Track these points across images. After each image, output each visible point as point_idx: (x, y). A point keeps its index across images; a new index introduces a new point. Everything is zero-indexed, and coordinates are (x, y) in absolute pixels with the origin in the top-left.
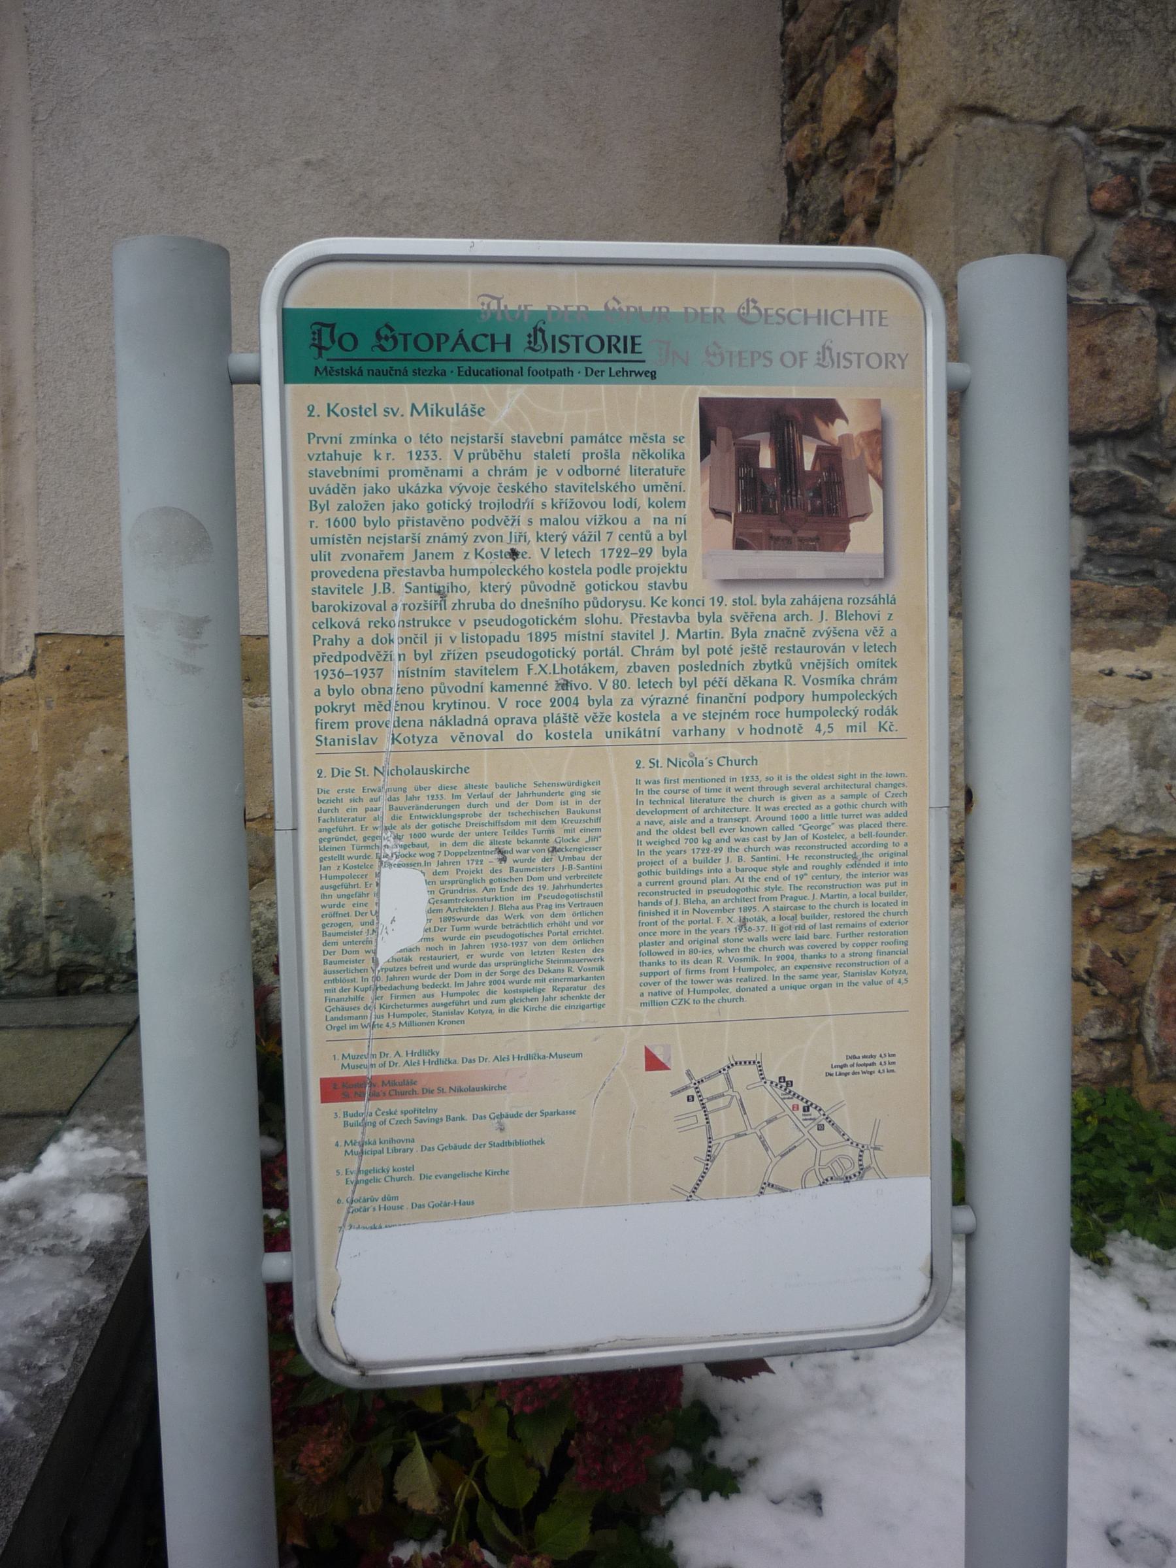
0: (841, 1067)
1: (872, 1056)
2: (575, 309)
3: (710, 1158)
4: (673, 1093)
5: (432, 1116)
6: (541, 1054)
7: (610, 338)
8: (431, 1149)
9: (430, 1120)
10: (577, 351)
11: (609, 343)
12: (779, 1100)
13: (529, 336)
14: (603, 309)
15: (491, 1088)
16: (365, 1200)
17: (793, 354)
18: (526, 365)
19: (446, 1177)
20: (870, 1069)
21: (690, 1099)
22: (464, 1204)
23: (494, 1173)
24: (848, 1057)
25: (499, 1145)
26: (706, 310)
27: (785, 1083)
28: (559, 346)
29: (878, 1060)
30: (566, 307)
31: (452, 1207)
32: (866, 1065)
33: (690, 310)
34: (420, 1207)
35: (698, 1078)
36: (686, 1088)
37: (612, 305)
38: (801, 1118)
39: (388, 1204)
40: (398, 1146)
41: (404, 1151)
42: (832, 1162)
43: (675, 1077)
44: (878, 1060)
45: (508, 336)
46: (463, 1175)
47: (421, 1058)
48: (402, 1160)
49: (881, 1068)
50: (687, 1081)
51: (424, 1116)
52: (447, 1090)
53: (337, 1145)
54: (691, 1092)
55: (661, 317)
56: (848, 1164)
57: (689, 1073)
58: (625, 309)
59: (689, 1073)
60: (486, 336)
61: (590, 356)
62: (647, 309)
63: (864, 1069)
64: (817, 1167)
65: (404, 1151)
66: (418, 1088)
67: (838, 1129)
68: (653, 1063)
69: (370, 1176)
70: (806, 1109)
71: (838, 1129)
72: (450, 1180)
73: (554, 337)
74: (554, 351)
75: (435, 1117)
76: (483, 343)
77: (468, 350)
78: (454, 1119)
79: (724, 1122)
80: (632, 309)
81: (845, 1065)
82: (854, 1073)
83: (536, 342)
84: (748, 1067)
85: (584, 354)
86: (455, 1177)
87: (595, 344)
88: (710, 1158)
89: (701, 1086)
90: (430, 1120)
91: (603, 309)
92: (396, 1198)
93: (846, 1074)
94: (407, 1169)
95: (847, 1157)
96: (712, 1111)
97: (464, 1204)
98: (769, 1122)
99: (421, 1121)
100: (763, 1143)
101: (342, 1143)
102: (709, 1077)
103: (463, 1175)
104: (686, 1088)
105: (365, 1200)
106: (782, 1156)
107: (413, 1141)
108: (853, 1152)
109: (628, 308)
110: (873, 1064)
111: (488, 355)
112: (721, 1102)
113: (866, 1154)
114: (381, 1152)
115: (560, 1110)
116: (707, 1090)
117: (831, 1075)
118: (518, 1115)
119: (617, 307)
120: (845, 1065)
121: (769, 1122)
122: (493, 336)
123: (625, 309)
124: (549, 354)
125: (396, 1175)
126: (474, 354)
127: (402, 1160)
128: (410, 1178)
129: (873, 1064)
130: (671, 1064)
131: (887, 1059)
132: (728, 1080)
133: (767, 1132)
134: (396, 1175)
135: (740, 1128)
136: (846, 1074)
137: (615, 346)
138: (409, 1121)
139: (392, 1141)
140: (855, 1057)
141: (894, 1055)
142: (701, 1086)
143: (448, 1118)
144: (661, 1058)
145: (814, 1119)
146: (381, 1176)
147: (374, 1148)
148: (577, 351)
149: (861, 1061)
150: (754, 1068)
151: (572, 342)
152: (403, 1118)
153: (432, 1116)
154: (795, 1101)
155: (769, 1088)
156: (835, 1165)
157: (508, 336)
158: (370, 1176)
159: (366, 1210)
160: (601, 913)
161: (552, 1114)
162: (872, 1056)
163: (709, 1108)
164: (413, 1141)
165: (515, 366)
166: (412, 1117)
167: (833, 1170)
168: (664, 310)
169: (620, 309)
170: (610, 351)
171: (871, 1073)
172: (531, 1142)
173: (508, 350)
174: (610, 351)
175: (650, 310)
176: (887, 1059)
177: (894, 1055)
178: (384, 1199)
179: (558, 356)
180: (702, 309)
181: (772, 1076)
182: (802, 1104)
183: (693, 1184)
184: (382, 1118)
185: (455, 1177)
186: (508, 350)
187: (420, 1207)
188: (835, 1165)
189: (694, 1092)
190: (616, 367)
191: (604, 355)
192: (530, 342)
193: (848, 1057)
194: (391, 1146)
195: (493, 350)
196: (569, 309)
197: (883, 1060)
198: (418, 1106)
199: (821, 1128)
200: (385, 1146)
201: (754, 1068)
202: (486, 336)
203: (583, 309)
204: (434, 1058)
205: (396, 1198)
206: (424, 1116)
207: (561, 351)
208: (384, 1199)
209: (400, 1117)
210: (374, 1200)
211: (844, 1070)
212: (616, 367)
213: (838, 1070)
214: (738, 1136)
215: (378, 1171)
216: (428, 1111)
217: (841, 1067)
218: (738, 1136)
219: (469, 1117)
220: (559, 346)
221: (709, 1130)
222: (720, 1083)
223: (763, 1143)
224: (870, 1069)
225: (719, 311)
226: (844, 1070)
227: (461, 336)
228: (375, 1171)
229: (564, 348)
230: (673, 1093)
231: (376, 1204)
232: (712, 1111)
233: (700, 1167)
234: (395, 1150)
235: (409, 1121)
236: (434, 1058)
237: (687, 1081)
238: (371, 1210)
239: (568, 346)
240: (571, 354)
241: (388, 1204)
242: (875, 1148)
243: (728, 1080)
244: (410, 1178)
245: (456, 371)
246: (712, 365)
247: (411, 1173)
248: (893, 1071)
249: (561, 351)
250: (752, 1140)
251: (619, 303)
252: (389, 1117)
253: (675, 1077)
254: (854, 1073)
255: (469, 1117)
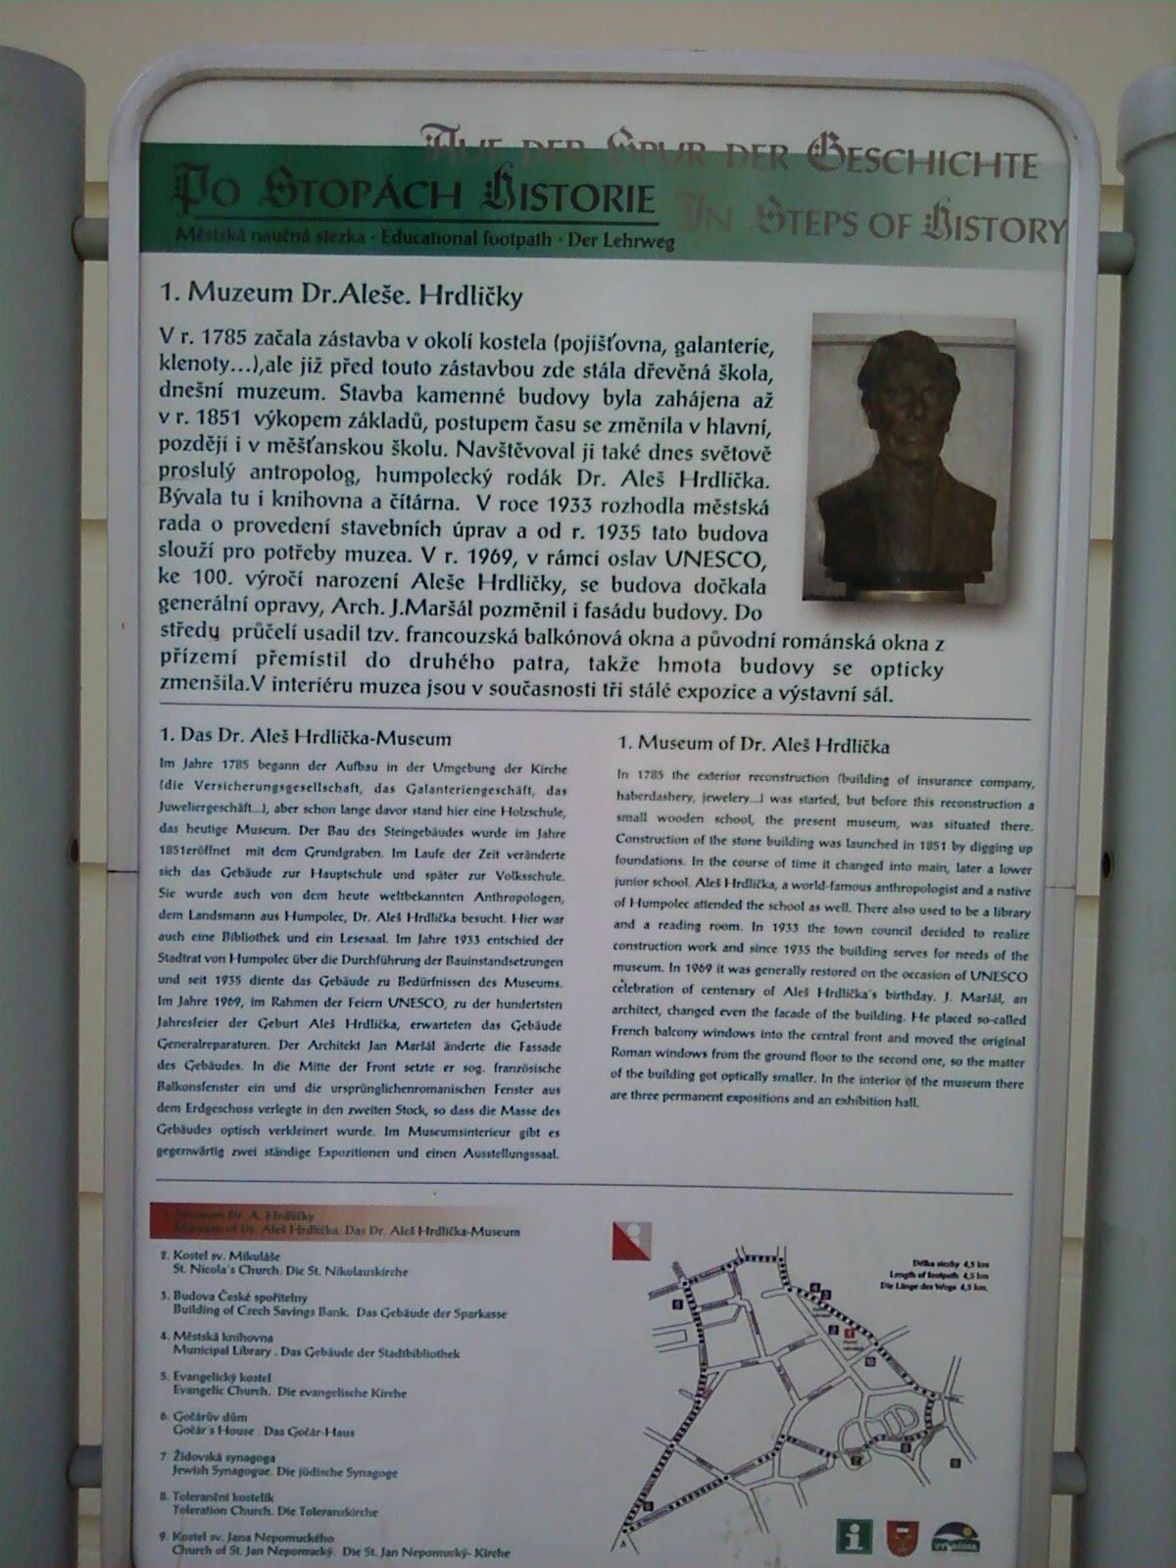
0: (905, 1276)
1: (952, 1264)
2: (564, 145)
3: (704, 1392)
4: (652, 1295)
5: (298, 1306)
6: (460, 1228)
7: (607, 188)
8: (296, 1353)
9: (295, 1312)
10: (559, 208)
11: (606, 196)
12: (808, 1316)
13: (489, 185)
14: (605, 146)
15: (386, 1273)
16: (200, 1418)
17: (890, 217)
18: (481, 229)
19: (316, 1393)
20: (949, 1282)
21: (677, 1305)
22: (341, 1434)
23: (384, 1394)
24: (916, 1263)
25: (392, 1355)
26: (760, 150)
27: (820, 1293)
28: (531, 200)
29: (961, 1270)
30: (551, 143)
31: (322, 1437)
32: (942, 1276)
33: (736, 149)
34: (277, 1433)
35: (690, 1274)
36: (672, 1288)
37: (620, 140)
38: (842, 1346)
39: (233, 1425)
40: (249, 1345)
41: (259, 1352)
42: (889, 1411)
43: (654, 1272)
44: (961, 1270)
45: (458, 186)
46: (340, 1393)
47: (288, 1224)
48: (250, 1365)
49: (966, 1283)
50: (673, 1279)
51: (289, 1306)
52: (321, 1270)
53: (164, 1336)
54: (680, 1294)
55: (692, 157)
56: (908, 1418)
57: (676, 1267)
58: (638, 147)
59: (676, 1267)
60: (424, 184)
61: (578, 216)
62: (672, 145)
63: (940, 1281)
64: (862, 1420)
65: (259, 1352)
66: (281, 1266)
67: (897, 1367)
68: (625, 1248)
69: (208, 1385)
70: (850, 1334)
71: (897, 1367)
72: (322, 1399)
73: (524, 187)
74: (524, 207)
75: (304, 1308)
76: (421, 195)
77: (397, 204)
78: (331, 1314)
79: (728, 1341)
80: (649, 147)
81: (912, 1275)
82: (925, 1287)
83: (498, 195)
84: (764, 1264)
85: (569, 212)
86: (328, 1395)
87: (585, 198)
88: (704, 1392)
89: (694, 1288)
90: (295, 1312)
91: (605, 146)
92: (244, 1418)
93: (913, 1288)
94: (260, 1378)
95: (915, 1414)
96: (710, 1326)
97: (341, 1434)
98: (793, 1347)
99: (284, 1312)
100: (784, 1377)
101: (170, 1335)
102: (708, 1275)
103: (340, 1393)
104: (672, 1288)
105: (200, 1418)
106: (812, 1398)
107: (271, 1339)
108: (920, 1403)
109: (643, 144)
110: (954, 1275)
111: (427, 211)
112: (728, 1312)
113: (937, 1407)
114: (225, 1351)
115: (485, 1311)
116: (704, 1293)
117: (890, 1287)
118: (423, 1314)
119: (626, 143)
120: (912, 1275)
121: (793, 1347)
122: (435, 185)
123: (638, 147)
124: (516, 213)
125: (244, 1385)
126: (405, 211)
127: (250, 1365)
128: (264, 1392)
129: (954, 1275)
130: (655, 1252)
131: (976, 1270)
132: (735, 1282)
133: (791, 1362)
134: (244, 1385)
135: (750, 1353)
136: (913, 1288)
137: (615, 201)
138: (266, 1311)
139: (241, 1337)
140: (926, 1263)
141: (987, 1265)
142: (694, 1288)
143: (322, 1310)
144: (637, 1242)
145: (862, 1350)
146: (224, 1385)
147: (214, 1345)
148: (559, 208)
149: (936, 1270)
150: (774, 1266)
151: (551, 193)
152: (259, 1306)
153: (298, 1306)
154: (834, 1320)
155: (797, 1300)
156: (889, 1417)
157: (458, 186)
158: (208, 1385)
159: (200, 1431)
160: (555, 1026)
161: (472, 1315)
162: (952, 1264)
163: (706, 1317)
164: (271, 1339)
165: (466, 230)
166: (270, 1305)
167: (885, 1423)
168: (697, 148)
169: (632, 146)
170: (607, 208)
171: (951, 1288)
172: (440, 1354)
173: (457, 205)
174: (607, 208)
175: (677, 148)
176: (976, 1270)
177: (987, 1265)
178: (227, 1418)
179: (530, 214)
180: (755, 147)
181: (801, 1278)
182: (843, 1326)
183: (676, 1429)
184: (228, 1304)
185: (328, 1395)
186: (457, 205)
187: (277, 1433)
188: (889, 1417)
189: (682, 1292)
190: (616, 232)
191: (599, 214)
192: (488, 194)
193: (916, 1263)
194: (239, 1345)
195: (434, 205)
196: (556, 145)
197: (969, 1271)
198: (280, 1291)
199: (870, 1362)
200: (231, 1344)
201: (774, 1266)
202: (424, 184)
203: (576, 146)
204: (305, 1224)
205: (244, 1418)
206: (289, 1306)
207: (535, 208)
208: (227, 1418)
209: (253, 1304)
210: (212, 1417)
211: (910, 1281)
212: (616, 232)
213: (901, 1280)
214: (746, 1364)
215: (219, 1378)
216: (293, 1298)
217: (905, 1276)
218: (746, 1364)
219: (351, 1311)
220: (531, 200)
221: (703, 1352)
222: (720, 1287)
223: (784, 1377)
224: (949, 1282)
225: (780, 150)
226: (910, 1281)
227: (389, 185)
228: (216, 1377)
229: (539, 203)
230: (652, 1295)
231: (214, 1424)
232: (710, 1326)
233: (689, 1405)
234: (245, 1351)
235: (266, 1311)
236: (305, 1224)
237: (673, 1279)
238: (207, 1432)
239: (545, 199)
240: (550, 212)
241: (233, 1425)
242: (952, 1399)
243: (735, 1282)
244: (264, 1392)
245: (379, 235)
246: (766, 231)
247: (266, 1385)
248: (983, 1288)
249: (535, 208)
250: (767, 1372)
251: (629, 136)
252: (238, 1304)
253: (654, 1272)
254: (925, 1287)
255: (351, 1311)
